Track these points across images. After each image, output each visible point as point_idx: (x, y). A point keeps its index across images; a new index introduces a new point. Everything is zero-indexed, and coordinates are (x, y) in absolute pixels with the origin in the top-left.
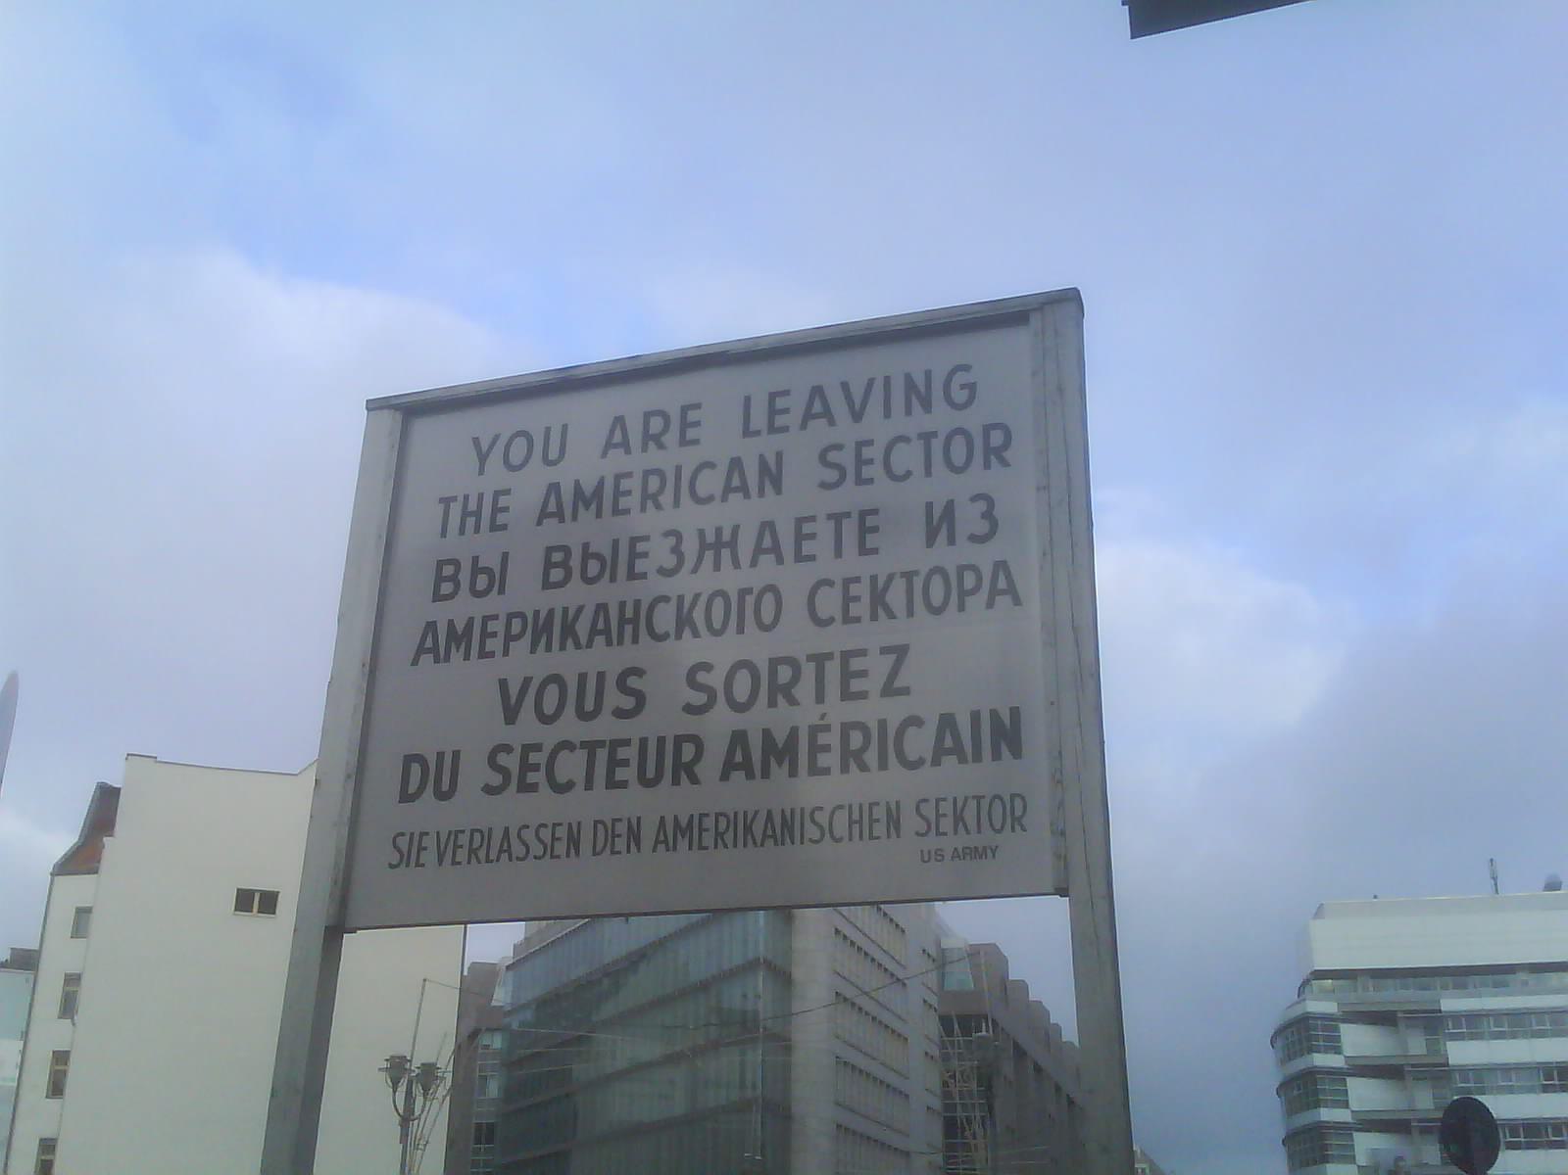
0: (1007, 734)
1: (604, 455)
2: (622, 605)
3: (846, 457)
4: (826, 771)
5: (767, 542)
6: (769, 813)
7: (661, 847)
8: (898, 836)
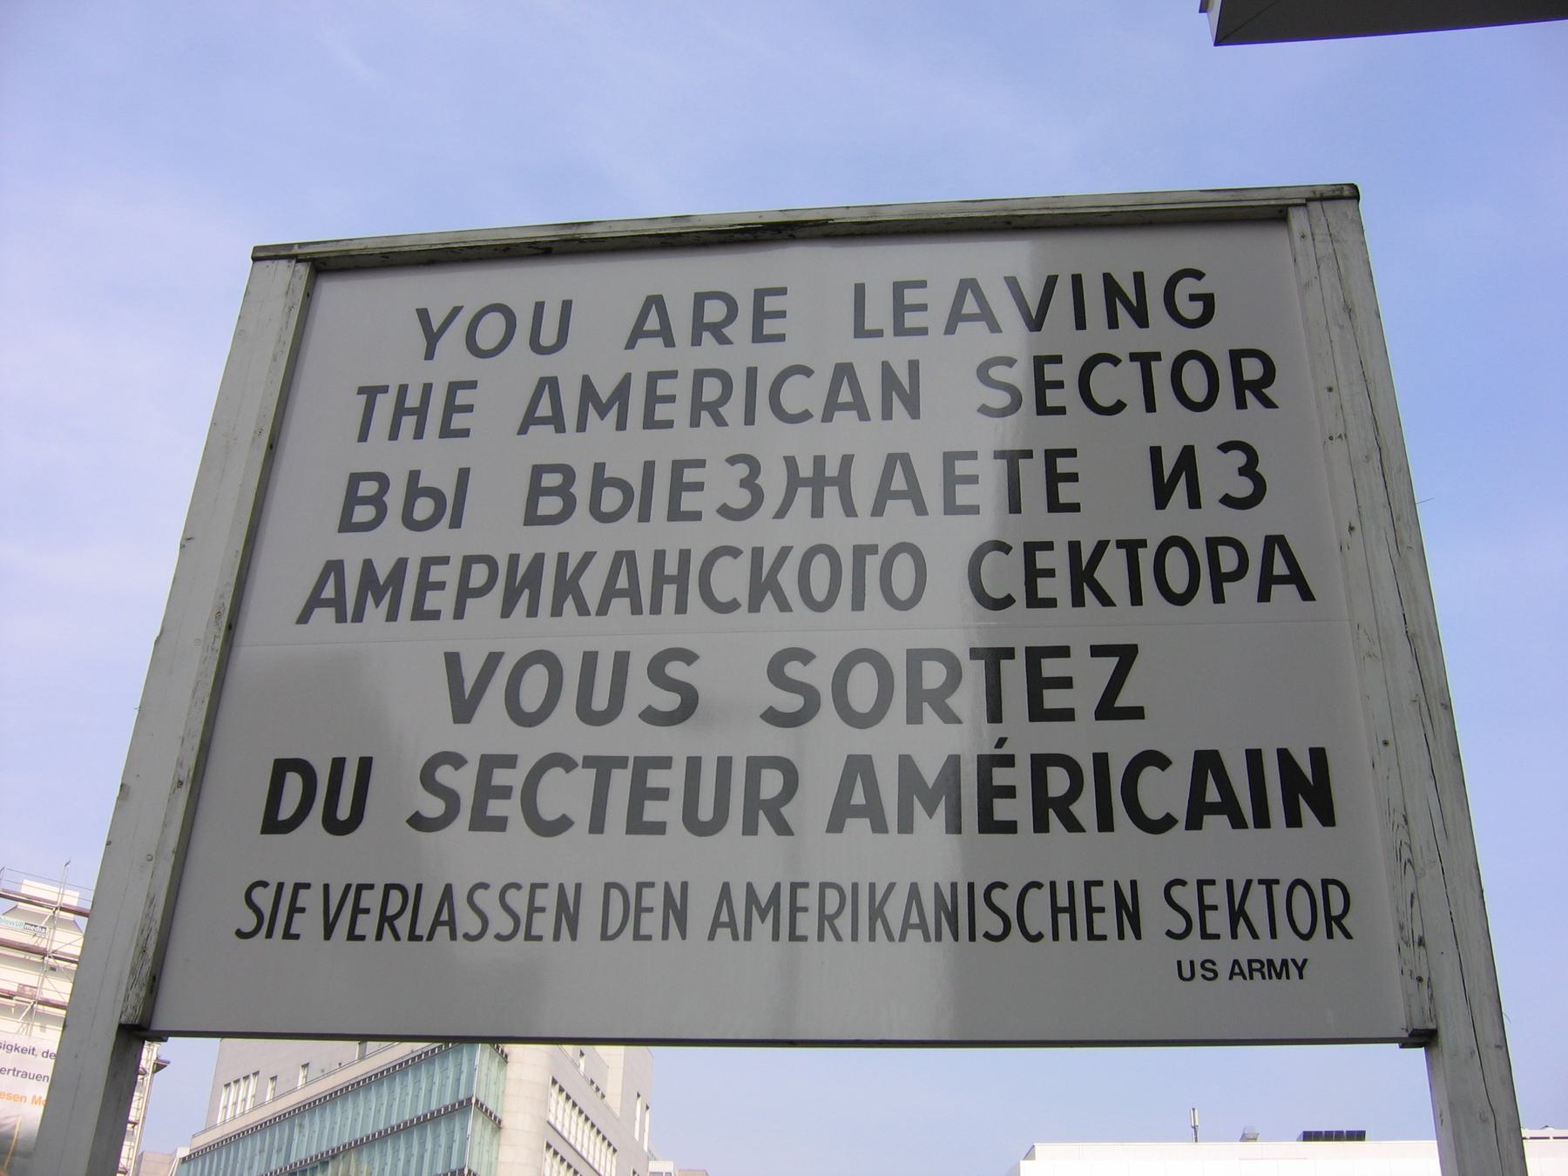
0: (1309, 789)
1: (631, 345)
2: (660, 556)
4: (1010, 827)
5: (898, 482)
7: (724, 934)
8: (1138, 936)
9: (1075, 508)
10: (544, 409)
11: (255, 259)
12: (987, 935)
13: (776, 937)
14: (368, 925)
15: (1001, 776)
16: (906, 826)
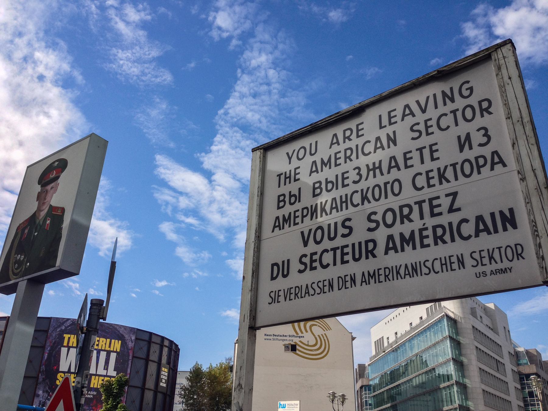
1: (330, 148)
2: (341, 197)
3: (422, 127)
4: (428, 246)
5: (393, 164)
6: (406, 265)
7: (364, 284)
8: (464, 268)
10: (314, 169)
12: (425, 274)
13: (375, 283)
14: (293, 296)
15: (425, 233)
16: (403, 250)
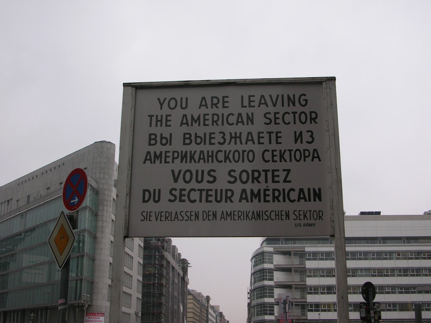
1: (200, 108)
2: (208, 152)
3: (272, 116)
4: (269, 201)
5: (250, 138)
6: (253, 212)
7: (223, 219)
9: (281, 143)
10: (185, 121)
11: (124, 86)
13: (231, 220)
14: (163, 218)
15: (267, 193)
16: (252, 201)
